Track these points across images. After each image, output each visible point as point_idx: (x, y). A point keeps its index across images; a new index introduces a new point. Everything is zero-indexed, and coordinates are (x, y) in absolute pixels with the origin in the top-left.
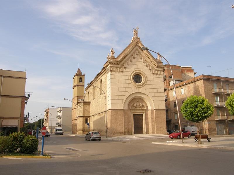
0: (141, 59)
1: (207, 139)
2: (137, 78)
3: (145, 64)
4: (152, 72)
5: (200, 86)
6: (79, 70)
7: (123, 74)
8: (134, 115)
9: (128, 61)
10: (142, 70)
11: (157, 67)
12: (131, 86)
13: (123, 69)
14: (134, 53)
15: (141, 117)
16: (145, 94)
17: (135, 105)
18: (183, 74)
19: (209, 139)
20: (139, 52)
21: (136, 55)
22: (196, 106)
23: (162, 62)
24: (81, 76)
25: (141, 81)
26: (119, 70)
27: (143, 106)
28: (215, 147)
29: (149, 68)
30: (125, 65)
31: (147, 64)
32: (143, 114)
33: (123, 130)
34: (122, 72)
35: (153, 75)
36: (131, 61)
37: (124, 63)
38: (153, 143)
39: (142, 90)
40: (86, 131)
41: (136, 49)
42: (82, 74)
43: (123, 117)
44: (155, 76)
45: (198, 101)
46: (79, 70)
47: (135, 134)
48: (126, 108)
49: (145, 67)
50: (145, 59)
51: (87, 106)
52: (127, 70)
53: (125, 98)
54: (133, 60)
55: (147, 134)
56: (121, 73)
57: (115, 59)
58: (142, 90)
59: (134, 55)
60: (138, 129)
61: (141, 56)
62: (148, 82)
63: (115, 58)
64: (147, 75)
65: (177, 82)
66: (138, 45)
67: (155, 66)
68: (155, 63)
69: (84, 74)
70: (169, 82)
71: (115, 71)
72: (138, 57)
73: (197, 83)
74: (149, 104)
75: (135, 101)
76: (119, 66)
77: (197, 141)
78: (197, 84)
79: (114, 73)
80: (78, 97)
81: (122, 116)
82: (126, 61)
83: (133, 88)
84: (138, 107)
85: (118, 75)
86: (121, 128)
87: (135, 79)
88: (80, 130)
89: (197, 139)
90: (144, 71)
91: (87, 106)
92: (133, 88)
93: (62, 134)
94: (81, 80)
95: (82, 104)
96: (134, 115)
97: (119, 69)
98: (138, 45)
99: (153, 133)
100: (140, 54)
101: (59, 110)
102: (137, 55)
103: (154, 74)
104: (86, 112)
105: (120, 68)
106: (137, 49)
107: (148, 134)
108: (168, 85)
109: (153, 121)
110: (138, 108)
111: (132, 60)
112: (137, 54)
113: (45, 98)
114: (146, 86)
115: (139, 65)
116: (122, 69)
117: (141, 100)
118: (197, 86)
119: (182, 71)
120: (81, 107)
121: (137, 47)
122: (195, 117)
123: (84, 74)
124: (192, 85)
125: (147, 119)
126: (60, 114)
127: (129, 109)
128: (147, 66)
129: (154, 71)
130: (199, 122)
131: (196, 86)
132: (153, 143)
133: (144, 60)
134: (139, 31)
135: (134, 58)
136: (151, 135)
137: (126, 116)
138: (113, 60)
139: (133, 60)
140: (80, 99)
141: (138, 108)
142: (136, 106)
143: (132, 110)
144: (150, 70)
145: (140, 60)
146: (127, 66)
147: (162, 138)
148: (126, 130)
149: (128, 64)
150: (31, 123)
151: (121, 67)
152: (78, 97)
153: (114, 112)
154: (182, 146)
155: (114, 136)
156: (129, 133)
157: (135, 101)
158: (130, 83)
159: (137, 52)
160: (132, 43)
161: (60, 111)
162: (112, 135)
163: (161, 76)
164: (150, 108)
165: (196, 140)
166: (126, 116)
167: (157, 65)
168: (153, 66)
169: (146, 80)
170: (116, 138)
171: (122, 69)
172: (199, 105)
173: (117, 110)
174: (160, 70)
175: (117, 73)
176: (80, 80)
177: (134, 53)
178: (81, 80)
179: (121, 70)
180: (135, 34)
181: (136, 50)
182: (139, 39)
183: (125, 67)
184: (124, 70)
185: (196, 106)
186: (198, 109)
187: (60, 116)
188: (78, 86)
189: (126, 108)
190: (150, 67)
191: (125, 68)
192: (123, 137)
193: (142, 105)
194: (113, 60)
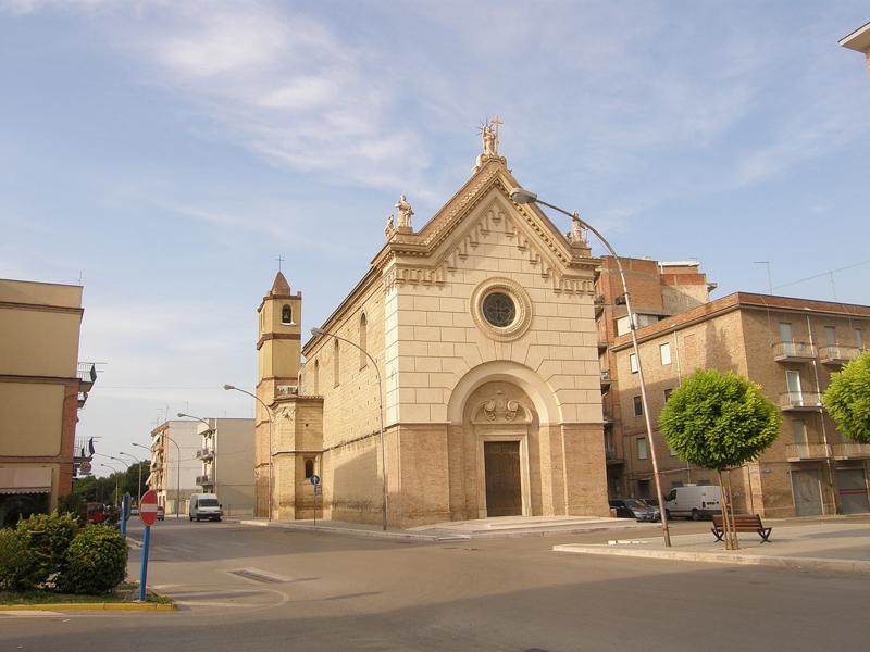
0: (510, 235)
1: (758, 531)
2: (497, 307)
3: (527, 255)
4: (550, 284)
5: (729, 336)
6: (280, 278)
7: (446, 291)
8: (487, 444)
9: (462, 246)
10: (514, 277)
11: (571, 266)
12: (475, 335)
13: (443, 275)
14: (484, 213)
15: (510, 453)
17: (490, 407)
18: (666, 293)
19: (764, 530)
20: (504, 211)
21: (490, 220)
22: (716, 411)
23: (588, 246)
24: (288, 302)
25: (513, 317)
26: (428, 279)
27: (520, 411)
28: (788, 562)
30: (450, 258)
32: (518, 443)
33: (444, 502)
34: (441, 284)
36: (475, 245)
37: (447, 253)
38: (557, 548)
39: (517, 352)
40: (308, 508)
41: (493, 197)
42: (293, 293)
43: (446, 453)
44: (564, 298)
45: (722, 392)
46: (280, 278)
47: (490, 515)
48: (457, 418)
49: (527, 267)
51: (310, 414)
52: (458, 277)
53: (452, 382)
54: (481, 239)
55: (534, 515)
56: (435, 290)
57: (414, 238)
58: (517, 352)
59: (484, 221)
60: (503, 496)
62: (538, 323)
63: (416, 235)
64: (536, 295)
65: (645, 321)
66: (498, 185)
67: (564, 260)
68: (563, 249)
69: (300, 293)
70: (615, 322)
71: (414, 282)
73: (720, 323)
74: (543, 404)
75: (492, 392)
76: (431, 262)
77: (720, 538)
78: (718, 329)
79: (409, 288)
80: (276, 378)
81: (442, 449)
82: (455, 245)
83: (480, 346)
84: (501, 415)
85: (427, 297)
86: (437, 492)
87: (491, 310)
88: (284, 504)
89: (720, 534)
90: (524, 281)
91: (310, 411)
92: (480, 346)
93: (216, 518)
94: (287, 314)
95: (294, 405)
96: (487, 444)
97: (428, 273)
98: (499, 185)
99: (558, 510)
100: (509, 218)
101: (204, 427)
102: (497, 220)
103: (558, 291)
104: (306, 434)
105: (433, 269)
106: (496, 198)
107: (541, 514)
108: (612, 331)
109: (556, 469)
110: (502, 421)
111: (477, 239)
112: (497, 216)
113: (155, 385)
114: (530, 338)
115: (501, 260)
116: (440, 273)
117: (513, 388)
118: (719, 335)
119: (664, 281)
120: (287, 416)
121: (496, 192)
122: (712, 449)
123: (300, 293)
124: (700, 332)
125: (534, 458)
126: (209, 444)
127: (468, 424)
128: (533, 262)
129: (557, 279)
130: (728, 467)
131: (714, 335)
132: (557, 548)
133: (522, 239)
134: (503, 132)
135: (486, 232)
136: (549, 519)
137: (458, 449)
138: (405, 240)
139: (481, 239)
140: (285, 387)
141: (502, 421)
142: (493, 413)
143: (477, 428)
144: (545, 276)
145: (506, 240)
146: (459, 262)
147: (592, 531)
148: (459, 502)
149: (464, 257)
150: (101, 478)
151: (439, 264)
152: (276, 378)
153: (410, 434)
154: (666, 557)
155: (413, 526)
156: (470, 514)
157: (492, 392)
158: (472, 324)
159: (496, 209)
160: (477, 176)
161: (209, 433)
162: (405, 520)
163: (562, 296)
164: (544, 419)
165: (717, 535)
166: (458, 449)
167: (569, 257)
168: (557, 260)
169: (529, 315)
170: (418, 530)
171: (439, 275)
172: (725, 405)
173: (420, 428)
174: (414, 267)
175: (422, 290)
176: (286, 317)
177: (484, 213)
178: (287, 314)
179: (438, 278)
180: (488, 143)
181: (491, 204)
182: (503, 162)
183: (452, 266)
184: (449, 277)
185: (716, 411)
186: (722, 422)
187: (210, 450)
188: (275, 336)
189: (457, 418)
190: (546, 267)
191: (453, 270)
192: (446, 526)
193: (515, 407)
194: (405, 240)
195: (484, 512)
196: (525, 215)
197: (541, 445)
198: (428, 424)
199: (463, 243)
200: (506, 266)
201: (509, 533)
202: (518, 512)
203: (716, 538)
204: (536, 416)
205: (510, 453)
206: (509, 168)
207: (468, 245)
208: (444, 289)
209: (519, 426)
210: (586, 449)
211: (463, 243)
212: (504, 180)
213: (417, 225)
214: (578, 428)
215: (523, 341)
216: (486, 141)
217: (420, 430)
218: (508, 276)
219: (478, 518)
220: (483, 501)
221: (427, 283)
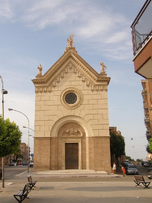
0: (75, 73)
2: (70, 97)
3: (81, 79)
4: (90, 88)
8: (66, 144)
9: (58, 78)
10: (77, 87)
11: (98, 81)
12: (61, 107)
13: (51, 88)
15: (75, 147)
16: (80, 117)
17: (67, 131)
19: (146, 183)
23: (106, 73)
25: (76, 100)
27: (78, 132)
29: (85, 83)
30: (54, 83)
31: (84, 78)
32: (78, 143)
33: (48, 164)
34: (50, 92)
35: (92, 92)
36: (62, 77)
37: (52, 81)
39: (76, 112)
43: (49, 147)
44: (95, 92)
48: (55, 135)
49: (81, 83)
50: (81, 72)
53: (52, 123)
54: (65, 75)
55: (82, 169)
56: (48, 94)
57: (42, 77)
58: (76, 112)
59: (66, 70)
60: (72, 161)
61: (75, 69)
62: (85, 102)
64: (84, 92)
66: (71, 57)
67: (95, 79)
71: (41, 92)
72: (72, 70)
74: (87, 130)
75: (68, 126)
81: (48, 146)
82: (55, 79)
84: (71, 134)
85: (46, 96)
86: (45, 160)
89: (138, 183)
90: (80, 88)
99: (90, 168)
100: (75, 67)
103: (93, 91)
105: (47, 87)
106: (70, 61)
107: (86, 169)
109: (90, 153)
110: (72, 136)
112: (71, 67)
115: (71, 82)
117: (77, 125)
121: (71, 59)
125: (84, 149)
129: (93, 86)
136: (88, 171)
137: (54, 146)
139: (65, 75)
141: (72, 136)
143: (63, 139)
144: (88, 86)
145: (74, 75)
147: (80, 177)
148: (53, 164)
149: (58, 82)
156: (58, 167)
157: (68, 126)
158: (60, 104)
159: (71, 65)
164: (87, 135)
165: (137, 183)
166: (54, 146)
167: (96, 78)
173: (41, 139)
175: (44, 94)
181: (69, 63)
182: (74, 49)
183: (54, 85)
184: (53, 89)
189: (55, 135)
190: (88, 82)
191: (54, 87)
193: (76, 131)
194: (39, 78)
195: (64, 167)
196: (81, 65)
197: (86, 144)
198: (43, 138)
199: (58, 77)
200: (73, 83)
201: (45, 176)
202: (77, 168)
203: (137, 185)
204: (84, 134)
205: (75, 147)
206: (76, 50)
207: (60, 78)
208: (51, 93)
209: (78, 138)
210: (102, 146)
211: (58, 77)
212: (72, 54)
213: (43, 73)
214: (99, 138)
215: (79, 108)
216: (69, 43)
217: (41, 140)
218: (74, 87)
219: (62, 169)
220: (64, 163)
221: (45, 92)
